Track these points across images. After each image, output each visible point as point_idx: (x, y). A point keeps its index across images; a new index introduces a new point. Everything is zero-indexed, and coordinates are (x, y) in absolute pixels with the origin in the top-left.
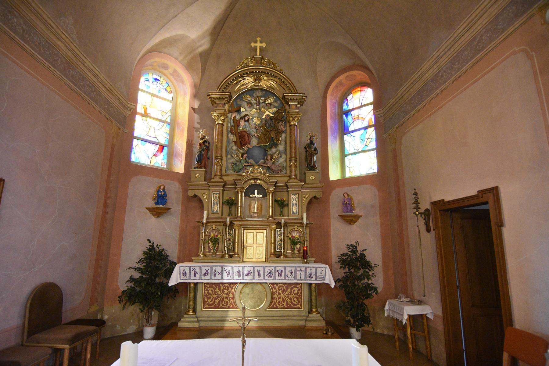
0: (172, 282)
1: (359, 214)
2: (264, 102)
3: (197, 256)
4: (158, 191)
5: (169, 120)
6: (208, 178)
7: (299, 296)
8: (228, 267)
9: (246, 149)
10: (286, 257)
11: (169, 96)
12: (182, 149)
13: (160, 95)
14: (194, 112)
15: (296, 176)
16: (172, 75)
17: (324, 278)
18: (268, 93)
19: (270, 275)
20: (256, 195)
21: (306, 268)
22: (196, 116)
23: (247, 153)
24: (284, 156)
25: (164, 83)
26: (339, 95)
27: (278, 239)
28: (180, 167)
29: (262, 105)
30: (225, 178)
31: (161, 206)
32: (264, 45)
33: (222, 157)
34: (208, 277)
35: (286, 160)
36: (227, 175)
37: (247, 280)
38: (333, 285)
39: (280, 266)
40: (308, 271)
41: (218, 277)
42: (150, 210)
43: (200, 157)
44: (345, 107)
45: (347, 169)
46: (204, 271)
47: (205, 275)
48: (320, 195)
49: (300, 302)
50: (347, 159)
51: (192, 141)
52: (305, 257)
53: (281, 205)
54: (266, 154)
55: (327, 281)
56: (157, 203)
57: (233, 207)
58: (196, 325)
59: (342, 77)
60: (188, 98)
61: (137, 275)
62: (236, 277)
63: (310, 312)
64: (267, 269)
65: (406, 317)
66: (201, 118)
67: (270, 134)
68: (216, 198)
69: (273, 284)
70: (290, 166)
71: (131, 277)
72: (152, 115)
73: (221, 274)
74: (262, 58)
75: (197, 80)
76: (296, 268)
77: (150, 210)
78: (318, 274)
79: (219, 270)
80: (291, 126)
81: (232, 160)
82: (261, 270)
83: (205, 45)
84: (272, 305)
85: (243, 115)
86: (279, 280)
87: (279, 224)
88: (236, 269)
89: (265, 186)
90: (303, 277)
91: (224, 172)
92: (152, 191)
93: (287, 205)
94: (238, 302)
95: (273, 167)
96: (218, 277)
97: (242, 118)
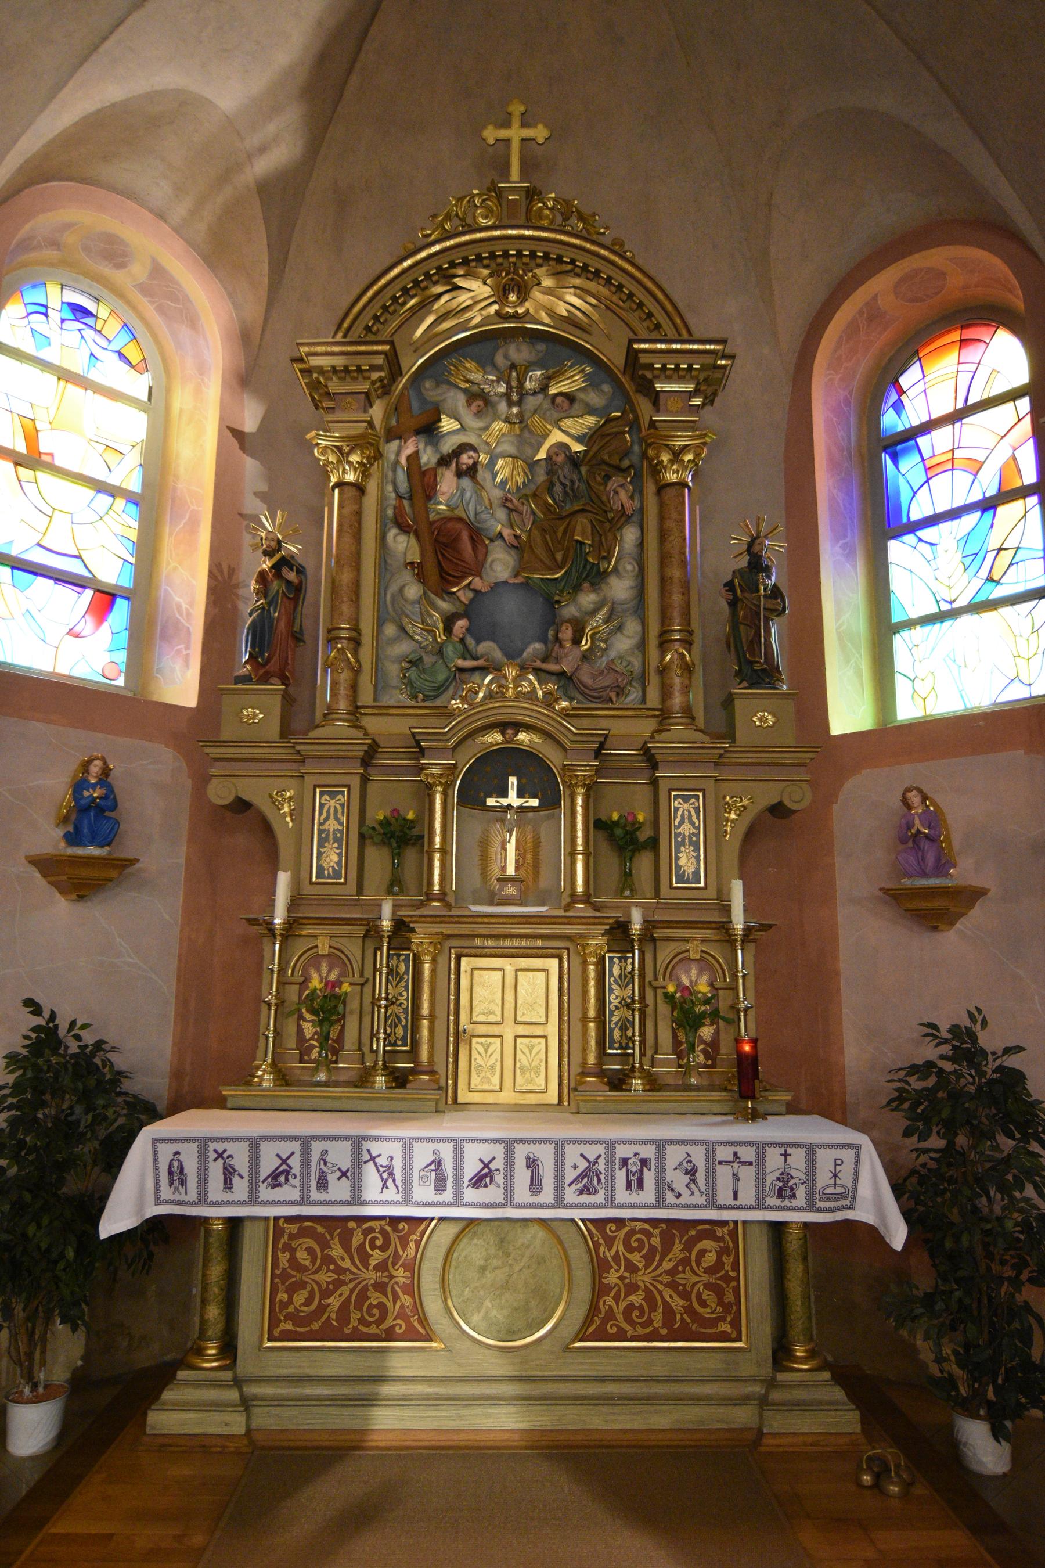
0: (117, 1219)
1: (976, 881)
2: (544, 388)
3: (246, 1077)
4: (79, 786)
5: (135, 485)
7: (725, 1282)
8: (388, 1139)
9: (465, 597)
10: (653, 1084)
11: (138, 385)
12: (192, 604)
13: (94, 376)
14: (242, 447)
15: (688, 712)
16: (144, 289)
17: (849, 1196)
18: (558, 347)
19: (588, 1180)
20: (513, 799)
21: (761, 1148)
22: (250, 465)
23: (466, 612)
24: (632, 627)
25: (113, 327)
26: (864, 365)
27: (613, 999)
28: (181, 683)
29: (531, 402)
30: (374, 725)
31: (92, 851)
32: (540, 133)
33: (356, 629)
34: (289, 1192)
35: (642, 645)
36: (382, 710)
37: (477, 1204)
38: (898, 1236)
39: (635, 1134)
40: (774, 1161)
41: (339, 1189)
42: (47, 866)
43: (261, 634)
44: (891, 421)
45: (902, 688)
46: (268, 1164)
47: (275, 1179)
48: (798, 798)
49: (732, 1310)
50: (900, 642)
51: (232, 571)
52: (746, 1086)
53: (626, 841)
54: (551, 618)
55: (863, 1214)
56: (73, 839)
57: (411, 855)
58: (235, 1424)
59: (881, 284)
60: (213, 390)
62: (424, 1192)
63: (781, 1353)
64: (572, 1154)
66: (271, 479)
67: (569, 530)
68: (333, 811)
70: (663, 671)
72: (58, 462)
73: (353, 1175)
74: (532, 194)
75: (254, 310)
76: (710, 1146)
77: (47, 866)
78: (823, 1179)
79: (340, 1156)
80: (662, 488)
81: (404, 648)
82: (546, 1155)
83: (278, 147)
84: (596, 1324)
85: (448, 446)
86: (634, 1205)
87: (619, 934)
88: (422, 1155)
89: (553, 757)
90: (747, 1195)
91: (366, 697)
92: (55, 785)
93: (653, 844)
94: (432, 1305)
95: (585, 676)
96: (339, 1189)
97: (444, 461)
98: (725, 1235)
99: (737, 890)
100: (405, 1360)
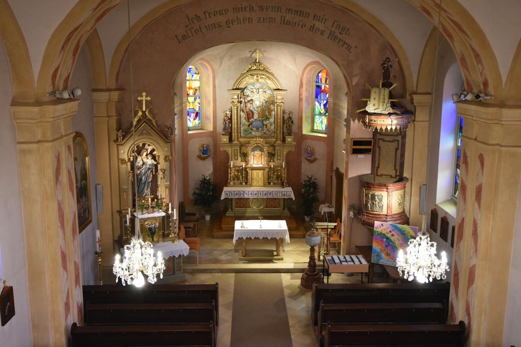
0: (223, 198)
6: (231, 140)
7: (279, 203)
17: (290, 196)
19: (266, 194)
24: (273, 125)
30: (240, 140)
37: (255, 197)
38: (294, 199)
40: (283, 193)
41: (242, 195)
45: (315, 124)
47: (236, 195)
49: (280, 206)
58: (233, 215)
61: (197, 191)
63: (284, 209)
65: (323, 213)
71: (194, 192)
73: (243, 194)
82: (262, 193)
84: (266, 207)
94: (251, 205)
95: (267, 132)
96: (242, 195)
99: (284, 163)
100: (248, 210)
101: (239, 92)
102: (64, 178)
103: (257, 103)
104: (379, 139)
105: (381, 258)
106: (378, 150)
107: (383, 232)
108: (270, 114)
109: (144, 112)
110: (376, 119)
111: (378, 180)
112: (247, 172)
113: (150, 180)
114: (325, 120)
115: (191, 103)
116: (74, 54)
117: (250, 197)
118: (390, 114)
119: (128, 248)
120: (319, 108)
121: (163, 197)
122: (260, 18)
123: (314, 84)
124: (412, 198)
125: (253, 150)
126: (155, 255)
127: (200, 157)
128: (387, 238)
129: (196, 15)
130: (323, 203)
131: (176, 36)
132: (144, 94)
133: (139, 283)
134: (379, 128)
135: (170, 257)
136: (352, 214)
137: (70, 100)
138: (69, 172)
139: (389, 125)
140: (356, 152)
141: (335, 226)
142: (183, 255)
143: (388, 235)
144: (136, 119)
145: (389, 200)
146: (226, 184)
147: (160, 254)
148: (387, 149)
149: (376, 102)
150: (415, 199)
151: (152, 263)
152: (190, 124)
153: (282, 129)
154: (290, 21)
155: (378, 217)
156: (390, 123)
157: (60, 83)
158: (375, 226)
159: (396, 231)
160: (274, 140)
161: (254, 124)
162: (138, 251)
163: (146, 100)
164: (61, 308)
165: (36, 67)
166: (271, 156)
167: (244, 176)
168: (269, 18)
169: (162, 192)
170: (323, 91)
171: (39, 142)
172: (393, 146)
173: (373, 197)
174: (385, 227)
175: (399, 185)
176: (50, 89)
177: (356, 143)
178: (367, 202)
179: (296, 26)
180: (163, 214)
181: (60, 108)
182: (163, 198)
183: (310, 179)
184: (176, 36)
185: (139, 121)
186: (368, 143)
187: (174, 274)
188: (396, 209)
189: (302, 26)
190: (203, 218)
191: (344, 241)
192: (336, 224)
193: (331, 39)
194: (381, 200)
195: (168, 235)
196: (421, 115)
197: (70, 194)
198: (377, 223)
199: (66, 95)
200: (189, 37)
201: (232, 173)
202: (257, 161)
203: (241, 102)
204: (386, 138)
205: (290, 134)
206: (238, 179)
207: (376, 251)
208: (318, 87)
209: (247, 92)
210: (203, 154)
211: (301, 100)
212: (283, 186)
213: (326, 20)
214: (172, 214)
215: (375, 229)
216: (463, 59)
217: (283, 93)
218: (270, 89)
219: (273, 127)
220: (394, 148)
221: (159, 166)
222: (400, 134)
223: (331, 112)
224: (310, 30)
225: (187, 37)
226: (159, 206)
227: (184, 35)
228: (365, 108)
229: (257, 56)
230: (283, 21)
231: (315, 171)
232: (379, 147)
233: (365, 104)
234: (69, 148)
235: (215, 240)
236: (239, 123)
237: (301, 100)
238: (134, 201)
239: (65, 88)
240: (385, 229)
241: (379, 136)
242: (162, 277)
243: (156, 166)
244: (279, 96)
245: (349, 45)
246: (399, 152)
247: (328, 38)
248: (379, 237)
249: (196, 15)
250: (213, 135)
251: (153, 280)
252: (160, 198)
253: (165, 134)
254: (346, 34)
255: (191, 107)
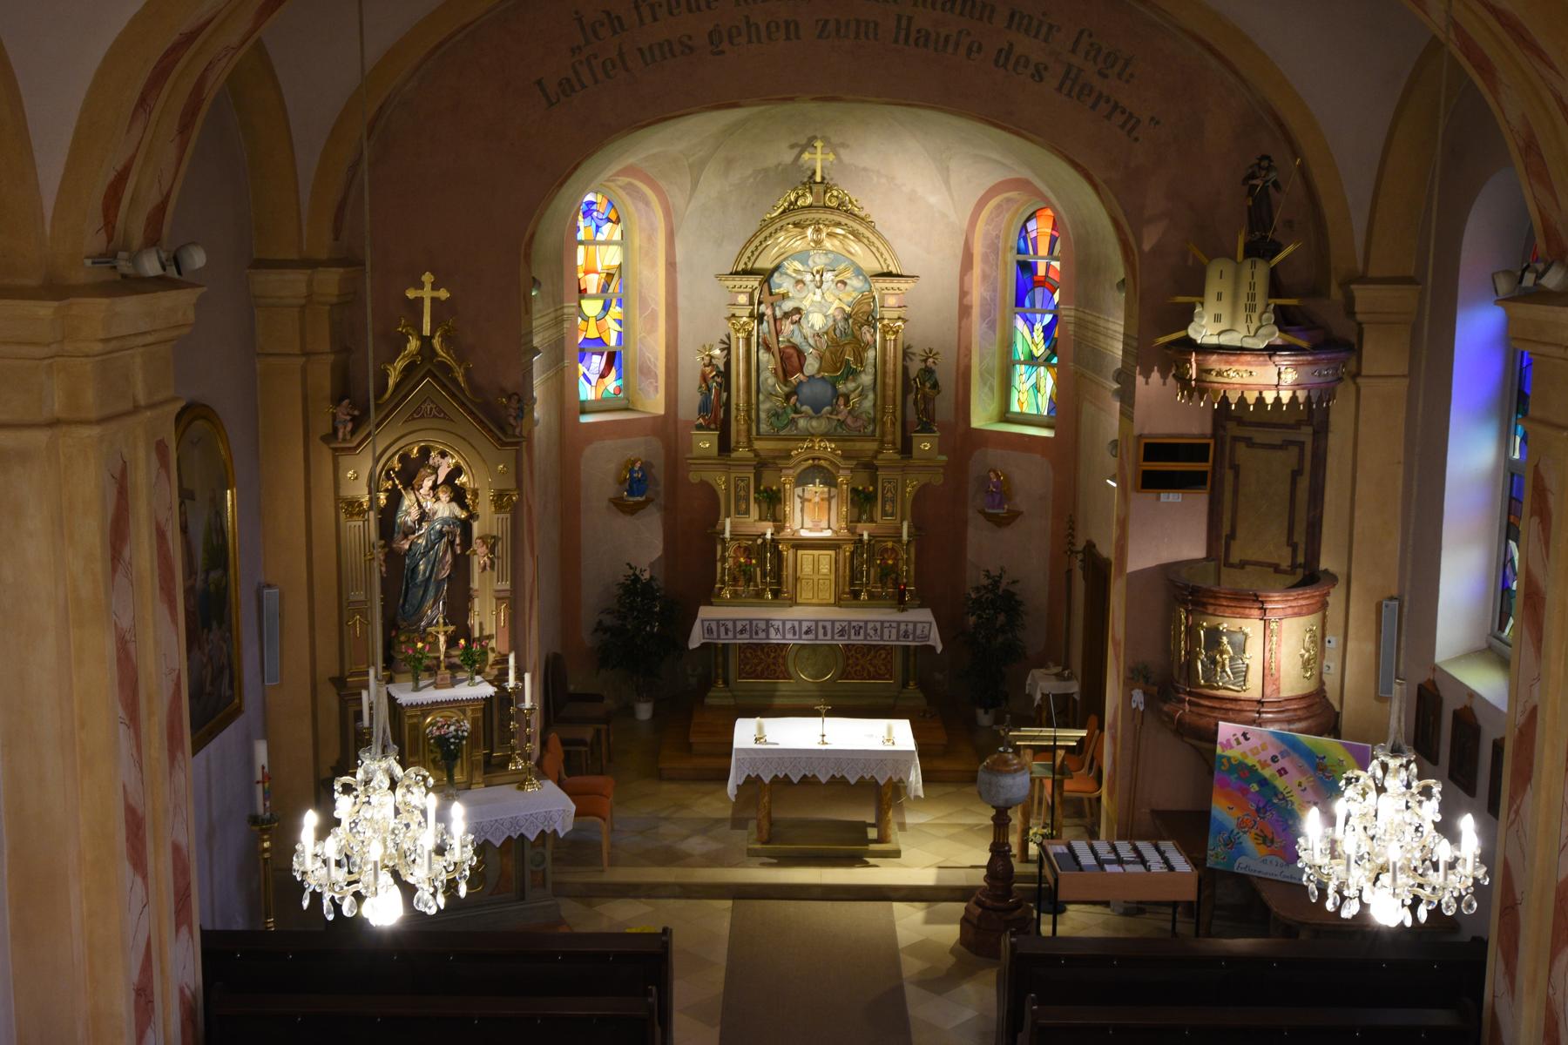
6: (725, 446)
17: (927, 637)
19: (842, 632)
21: (899, 623)
24: (871, 396)
30: (758, 445)
34: (746, 636)
38: (939, 649)
40: (903, 627)
45: (1015, 396)
46: (739, 627)
47: (741, 632)
58: (732, 702)
61: (608, 620)
62: (789, 636)
65: (1038, 696)
69: (847, 646)
71: (600, 622)
73: (767, 631)
76: (882, 622)
78: (918, 632)
82: (829, 626)
84: (845, 674)
90: (894, 637)
94: (792, 669)
95: (849, 421)
98: (889, 650)
100: (783, 685)
101: (753, 282)
102: (142, 551)
103: (817, 321)
104: (1235, 439)
105: (1241, 852)
106: (1229, 476)
107: (1251, 761)
108: (860, 359)
109: (426, 342)
110: (1224, 368)
111: (1232, 580)
112: (779, 556)
113: (445, 573)
114: (1048, 381)
115: (592, 321)
116: (185, 127)
117: (790, 640)
118: (1272, 350)
119: (348, 789)
120: (1029, 339)
121: (486, 633)
122: (827, 22)
123: (1012, 258)
124: (1350, 645)
125: (802, 481)
126: (443, 816)
127: (619, 505)
128: (1264, 782)
129: (608, 14)
130: (1041, 665)
131: (539, 83)
132: (427, 278)
133: (384, 911)
134: (1233, 397)
135: (510, 837)
136: (1138, 696)
137: (161, 283)
138: (161, 535)
139: (1268, 387)
140: (1153, 482)
141: (1081, 741)
142: (555, 831)
143: (1267, 773)
144: (400, 364)
145: (1270, 649)
146: (708, 596)
147: (458, 810)
148: (1265, 472)
149: (1224, 308)
150: (1360, 649)
151: (428, 840)
152: (587, 392)
153: (897, 412)
154: (928, 35)
155: (1233, 709)
156: (1273, 380)
157: (134, 224)
158: (1221, 738)
159: (1296, 756)
160: (874, 446)
161: (806, 391)
162: (383, 802)
163: (433, 300)
164: (122, 1006)
165: (50, 172)
166: (862, 502)
167: (769, 569)
168: (858, 22)
169: (486, 617)
170: (1042, 283)
171: (54, 423)
172: (1283, 462)
173: (1214, 636)
174: (1254, 741)
175: (1303, 598)
176: (95, 242)
177: (1155, 450)
178: (1192, 656)
179: (950, 49)
180: (488, 690)
181: (130, 307)
182: (490, 637)
183: (996, 583)
184: (539, 83)
185: (408, 370)
186: (1194, 451)
187: (523, 899)
188: (1292, 681)
189: (970, 50)
190: (630, 711)
191: (1111, 793)
192: (1083, 733)
193: (1069, 94)
194: (1241, 649)
195: (503, 764)
196: (1382, 357)
197: (163, 610)
198: (1226, 730)
199: (151, 265)
200: (584, 87)
201: (729, 559)
202: (812, 517)
203: (761, 318)
204: (1260, 436)
205: (926, 428)
206: (750, 579)
207: (1222, 828)
208: (1026, 267)
209: (782, 284)
210: (631, 493)
211: (964, 311)
212: (901, 603)
213: (1051, 27)
214: (519, 692)
215: (1219, 750)
216: (1530, 147)
217: (903, 285)
218: (859, 271)
219: (868, 404)
220: (1289, 471)
221: (476, 527)
222: (1307, 421)
223: (1070, 352)
224: (996, 62)
225: (578, 87)
226: (472, 661)
227: (568, 80)
228: (1186, 328)
229: (818, 159)
230: (903, 33)
231: (1014, 554)
232: (1236, 469)
233: (1186, 316)
234: (161, 448)
235: (666, 787)
236: (753, 387)
237: (964, 311)
238: (389, 646)
239: (152, 241)
240: (1255, 751)
241: (1233, 429)
242: (463, 890)
243: (466, 526)
244: (890, 297)
245: (1131, 115)
246: (1304, 483)
247: (1059, 89)
248: (1233, 778)
249: (608, 14)
250: (666, 428)
251: (431, 903)
252: (477, 634)
253: (496, 413)
254: (1119, 76)
255: (593, 333)
